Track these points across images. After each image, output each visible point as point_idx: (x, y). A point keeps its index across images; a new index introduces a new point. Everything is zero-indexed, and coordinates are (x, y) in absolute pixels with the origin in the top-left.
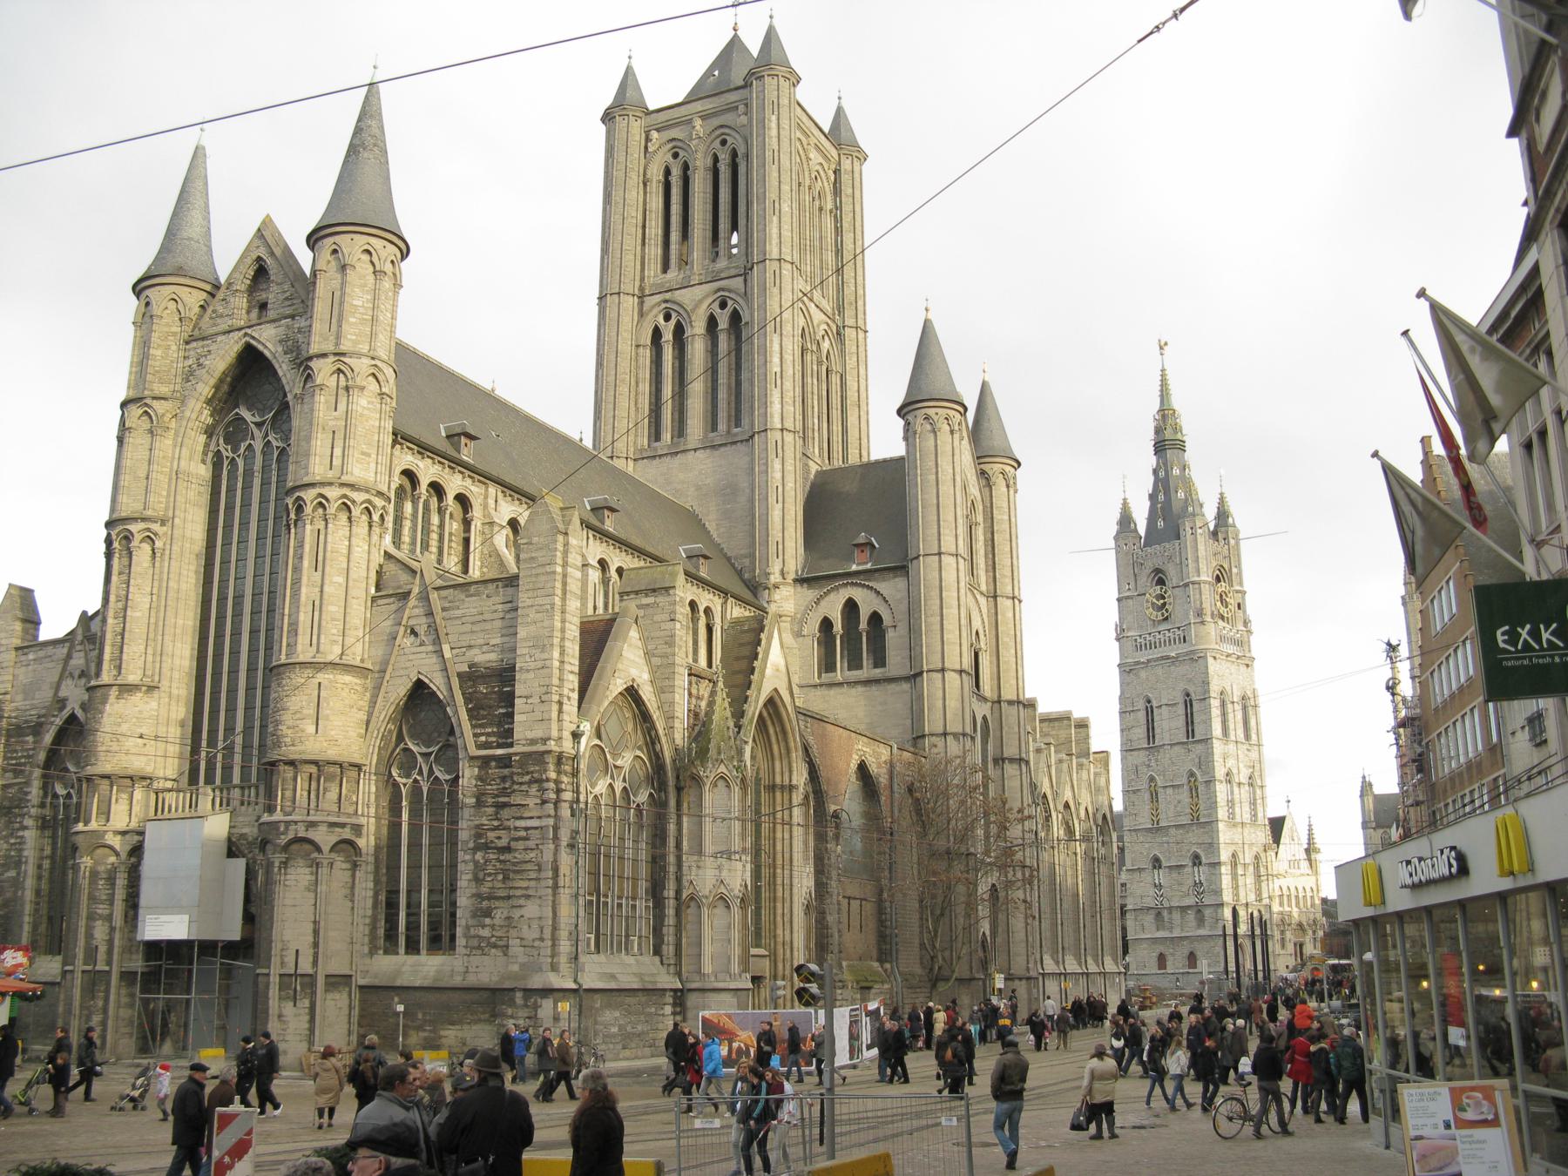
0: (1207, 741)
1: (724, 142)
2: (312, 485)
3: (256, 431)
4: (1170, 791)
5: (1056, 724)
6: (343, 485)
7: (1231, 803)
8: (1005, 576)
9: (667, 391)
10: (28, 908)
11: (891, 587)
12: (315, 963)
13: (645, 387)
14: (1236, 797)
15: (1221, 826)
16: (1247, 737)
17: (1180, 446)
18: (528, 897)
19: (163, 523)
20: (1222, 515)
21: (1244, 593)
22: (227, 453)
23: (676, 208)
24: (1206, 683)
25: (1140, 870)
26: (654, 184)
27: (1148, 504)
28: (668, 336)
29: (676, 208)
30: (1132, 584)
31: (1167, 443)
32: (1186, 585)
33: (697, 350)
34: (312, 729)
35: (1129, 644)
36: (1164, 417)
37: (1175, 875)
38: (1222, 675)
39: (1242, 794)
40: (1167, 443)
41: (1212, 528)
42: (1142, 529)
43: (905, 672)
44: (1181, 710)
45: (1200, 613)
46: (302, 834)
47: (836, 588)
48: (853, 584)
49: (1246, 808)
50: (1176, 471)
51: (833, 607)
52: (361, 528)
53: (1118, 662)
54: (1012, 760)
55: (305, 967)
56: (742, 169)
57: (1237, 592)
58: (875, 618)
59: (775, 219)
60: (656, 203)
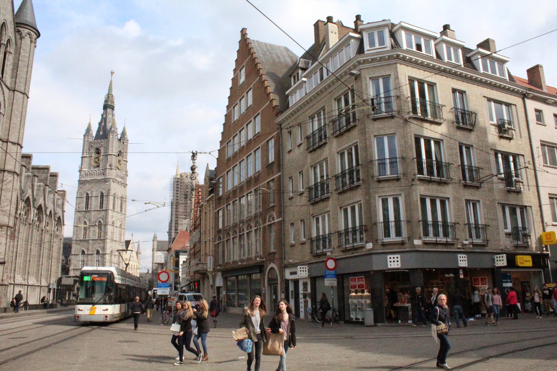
0: (106, 210)
5: (42, 171)
7: (113, 233)
8: (20, 82)
14: (115, 231)
15: (108, 241)
16: (121, 211)
21: (127, 162)
24: (109, 190)
25: (76, 255)
31: (108, 106)
32: (107, 155)
38: (115, 188)
41: (119, 138)
42: (94, 134)
45: (110, 166)
49: (118, 236)
53: (78, 179)
54: (9, 172)
57: (125, 161)
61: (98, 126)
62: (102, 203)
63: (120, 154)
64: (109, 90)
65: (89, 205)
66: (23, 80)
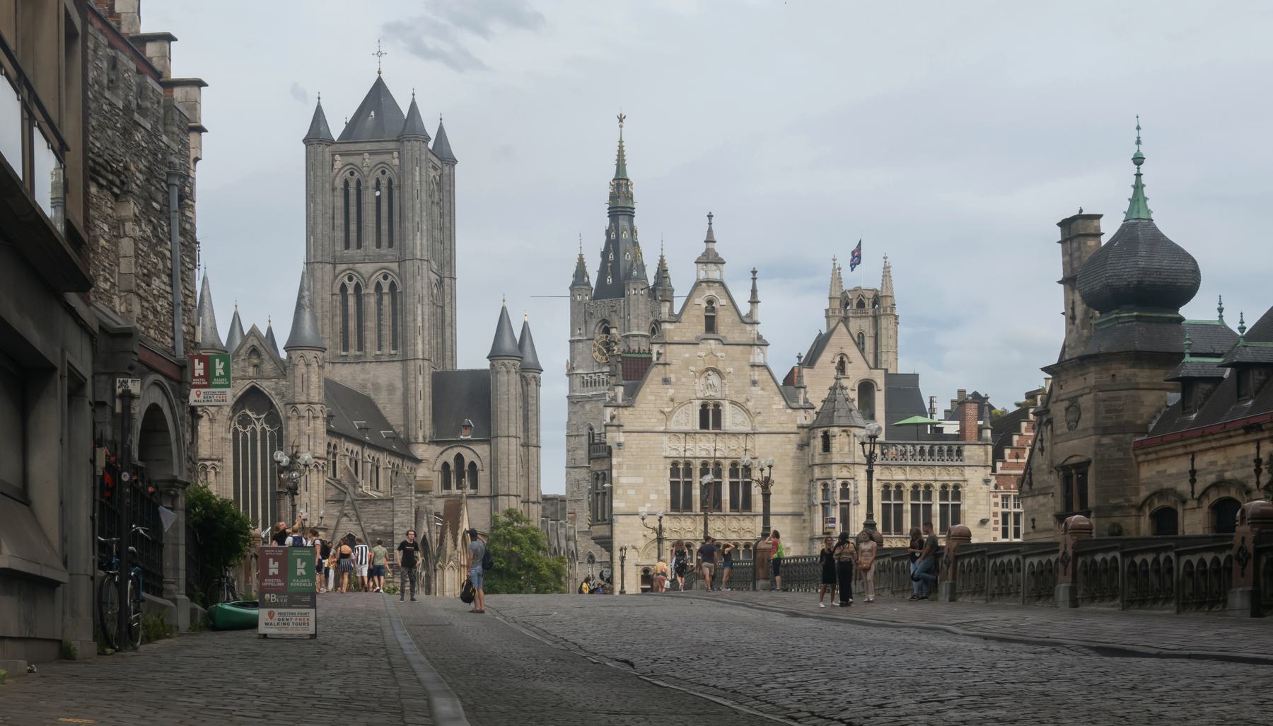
1: (383, 172)
3: (256, 422)
8: (532, 435)
9: (352, 324)
11: (482, 450)
13: (338, 319)
17: (630, 213)
19: (219, 461)
20: (662, 272)
22: (240, 429)
26: (338, 190)
28: (351, 291)
35: (577, 381)
36: (618, 185)
42: (593, 281)
43: (487, 493)
50: (628, 257)
51: (450, 456)
52: (321, 474)
56: (396, 193)
58: (472, 465)
59: (418, 234)
60: (340, 202)
64: (618, 166)
66: (534, 433)
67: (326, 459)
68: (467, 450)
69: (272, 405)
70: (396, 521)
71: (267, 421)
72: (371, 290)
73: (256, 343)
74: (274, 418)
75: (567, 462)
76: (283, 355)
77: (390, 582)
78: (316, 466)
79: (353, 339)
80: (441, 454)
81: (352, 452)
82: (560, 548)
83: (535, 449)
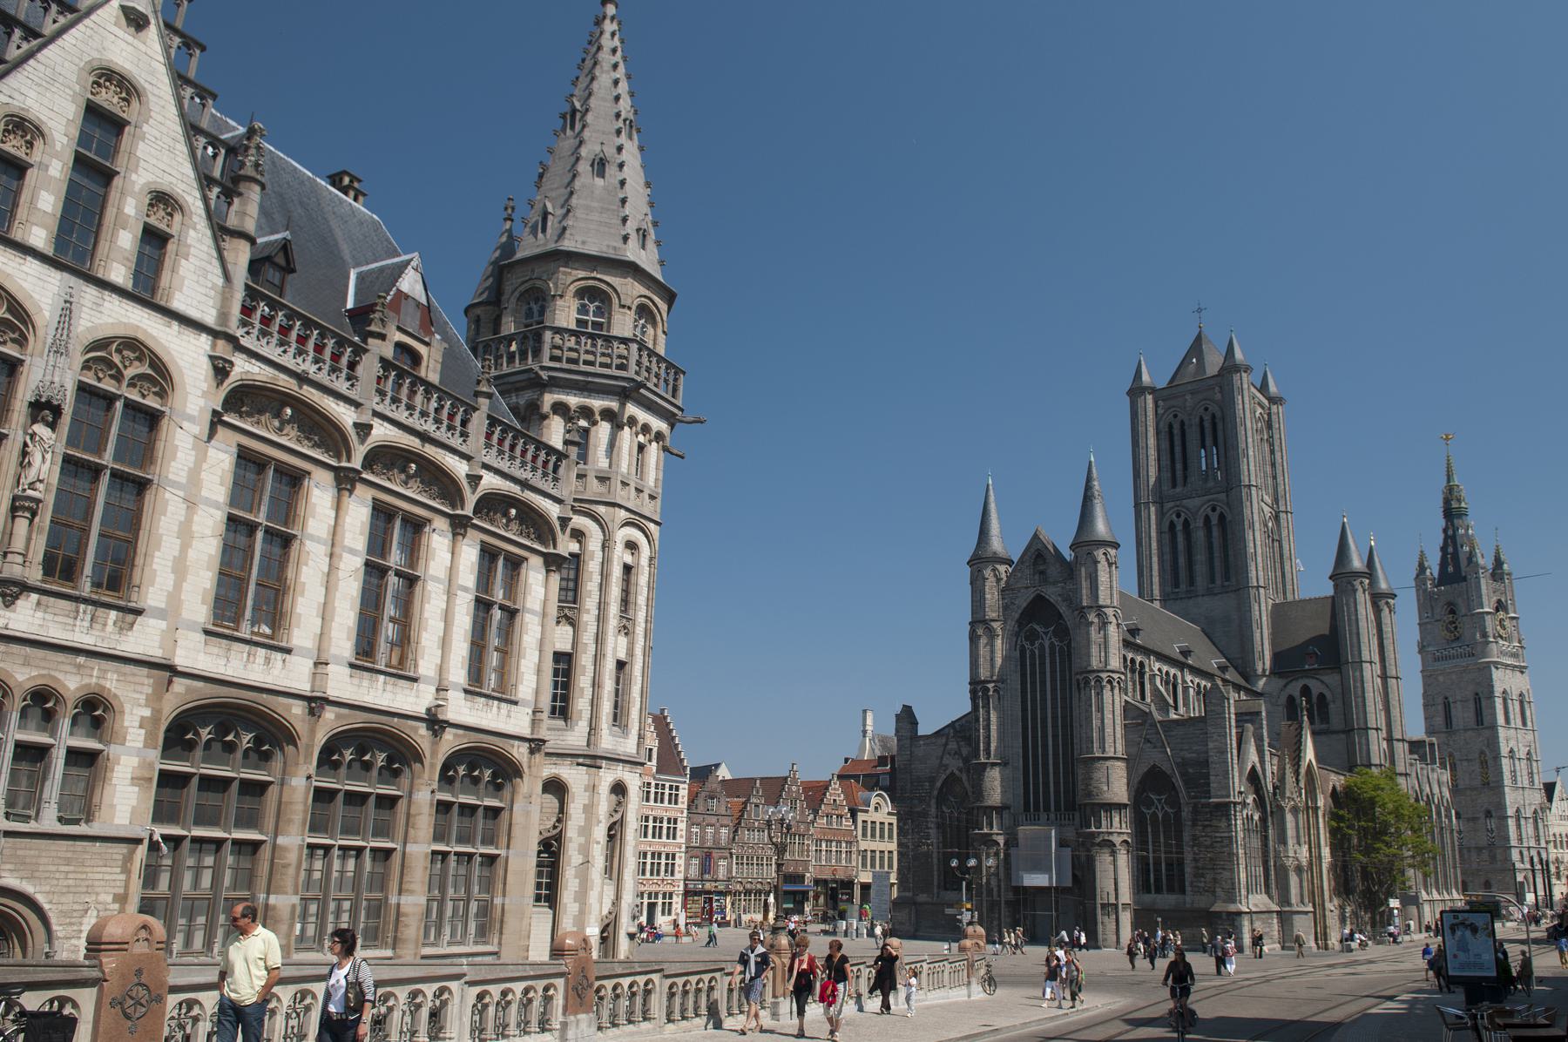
0: (1493, 727)
1: (1206, 409)
2: (1094, 671)
4: (1465, 763)
6: (1108, 671)
9: (1182, 560)
10: (935, 868)
11: (1332, 679)
12: (1117, 898)
14: (1518, 768)
15: (1507, 789)
16: (1524, 724)
17: (1461, 514)
18: (1224, 869)
23: (1178, 449)
27: (1440, 554)
28: (1179, 527)
29: (1178, 449)
30: (1430, 611)
33: (1199, 536)
34: (1105, 788)
37: (1471, 824)
39: (1522, 767)
40: (1452, 513)
44: (1471, 705)
46: (1106, 838)
47: (1296, 679)
48: (1307, 677)
49: (1526, 777)
51: (1295, 689)
52: (1116, 691)
55: (1112, 900)
56: (1220, 426)
58: (1322, 696)
59: (1245, 460)
61: (1439, 555)
62: (1479, 713)
63: (1500, 606)
65: (1454, 720)
67: (1122, 673)
68: (1315, 681)
69: (1060, 616)
70: (1211, 745)
71: (1055, 633)
72: (1200, 523)
73: (1040, 546)
74: (1063, 633)
75: (1426, 729)
76: (1068, 555)
77: (1207, 826)
78: (1109, 682)
79: (1183, 574)
80: (1285, 686)
81: (1167, 673)
82: (1433, 795)
83: (1394, 681)
